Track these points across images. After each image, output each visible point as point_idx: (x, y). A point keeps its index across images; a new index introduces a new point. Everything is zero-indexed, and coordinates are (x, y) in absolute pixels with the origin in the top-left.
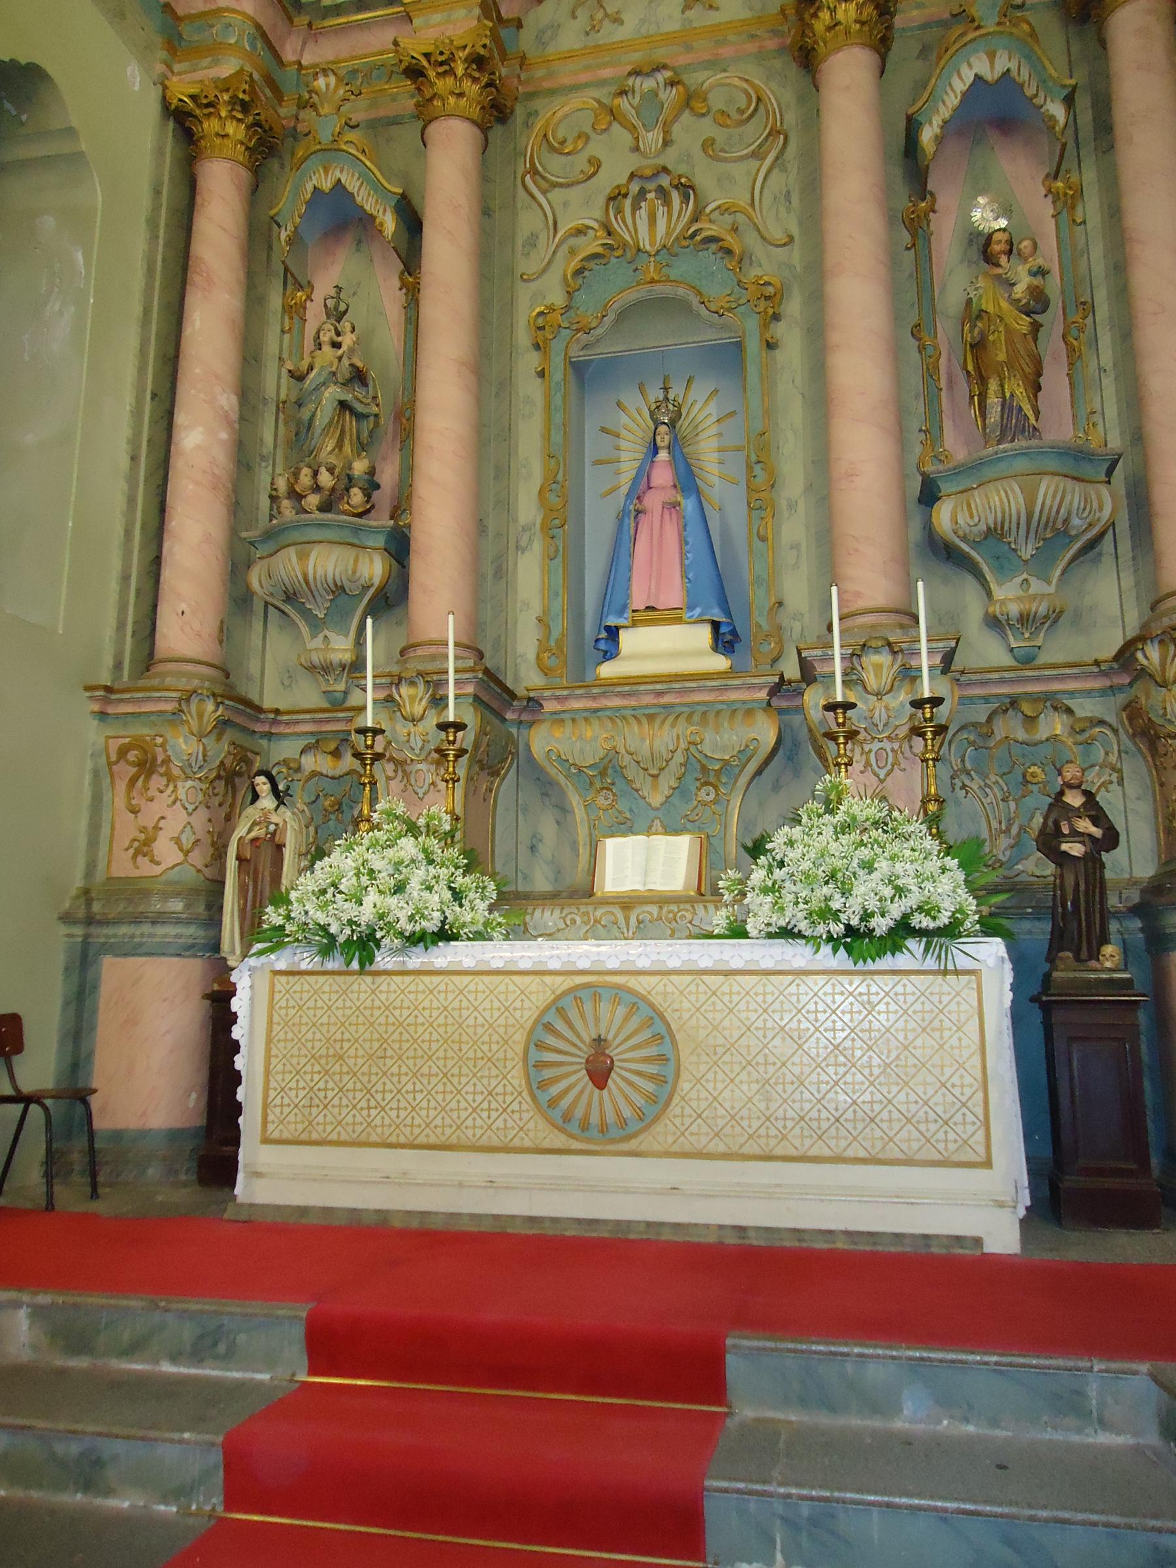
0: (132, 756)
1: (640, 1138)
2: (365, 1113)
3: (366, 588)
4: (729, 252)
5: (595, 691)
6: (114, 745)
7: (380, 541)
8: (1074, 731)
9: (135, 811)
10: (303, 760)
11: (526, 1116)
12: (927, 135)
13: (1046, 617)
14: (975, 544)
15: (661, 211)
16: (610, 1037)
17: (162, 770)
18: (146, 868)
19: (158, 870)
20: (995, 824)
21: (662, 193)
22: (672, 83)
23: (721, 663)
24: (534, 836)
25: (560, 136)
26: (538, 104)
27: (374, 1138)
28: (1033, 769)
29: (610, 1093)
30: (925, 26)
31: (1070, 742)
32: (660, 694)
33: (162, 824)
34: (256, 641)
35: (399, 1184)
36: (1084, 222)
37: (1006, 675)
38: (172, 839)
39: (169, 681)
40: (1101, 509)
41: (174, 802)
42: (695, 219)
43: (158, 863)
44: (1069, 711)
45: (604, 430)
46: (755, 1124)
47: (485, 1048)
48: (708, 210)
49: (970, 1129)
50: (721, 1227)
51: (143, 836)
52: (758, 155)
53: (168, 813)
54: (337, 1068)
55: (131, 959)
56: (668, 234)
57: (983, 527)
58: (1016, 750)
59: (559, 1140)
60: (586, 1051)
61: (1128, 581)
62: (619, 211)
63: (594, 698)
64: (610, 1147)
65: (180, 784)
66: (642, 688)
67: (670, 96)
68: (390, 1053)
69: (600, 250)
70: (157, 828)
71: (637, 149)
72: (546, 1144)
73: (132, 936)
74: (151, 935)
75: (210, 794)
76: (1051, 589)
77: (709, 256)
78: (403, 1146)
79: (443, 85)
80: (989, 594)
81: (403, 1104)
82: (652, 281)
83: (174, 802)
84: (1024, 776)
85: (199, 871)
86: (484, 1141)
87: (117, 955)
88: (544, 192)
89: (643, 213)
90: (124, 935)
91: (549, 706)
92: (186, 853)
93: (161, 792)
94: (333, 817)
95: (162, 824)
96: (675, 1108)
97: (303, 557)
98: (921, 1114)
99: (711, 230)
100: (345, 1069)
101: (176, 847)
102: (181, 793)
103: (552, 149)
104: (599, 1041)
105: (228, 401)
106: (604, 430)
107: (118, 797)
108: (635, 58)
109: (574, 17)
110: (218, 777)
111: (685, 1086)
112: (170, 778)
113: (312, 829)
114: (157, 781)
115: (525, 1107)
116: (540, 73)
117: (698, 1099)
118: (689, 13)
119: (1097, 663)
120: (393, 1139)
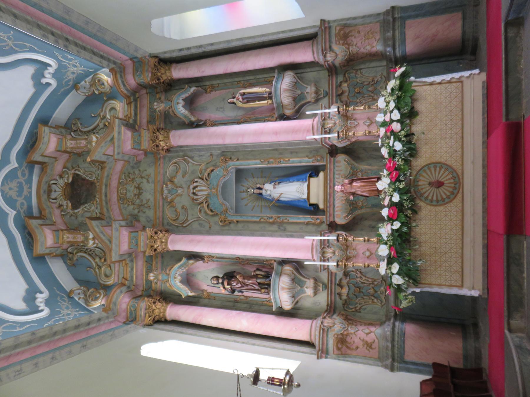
0: (340, 346)
1: (459, 173)
2: (453, 254)
3: (293, 273)
4: (212, 171)
5: (328, 205)
6: (336, 352)
7: (280, 267)
8: (346, 81)
9: (357, 348)
10: (343, 299)
11: (452, 205)
12: (193, 119)
13: (316, 88)
14: (296, 105)
15: (199, 188)
16: (429, 181)
17: (345, 336)
19: (376, 341)
20: (371, 100)
21: (195, 188)
22: (167, 185)
23: (321, 174)
24: (369, 227)
25: (174, 216)
26: (165, 222)
27: (460, 251)
28: (356, 91)
29: (444, 181)
30: (165, 123)
31: (349, 82)
32: (330, 187)
33: (362, 338)
35: (474, 242)
36: (218, 84)
37: (331, 97)
38: (367, 336)
40: (290, 75)
41: (355, 334)
42: (203, 179)
43: (374, 341)
44: (341, 82)
45: (252, 210)
46: (453, 141)
47: (432, 217)
48: (200, 176)
49: (452, 87)
50: (483, 148)
51: (366, 345)
52: (188, 163)
53: (358, 336)
54: (439, 263)
55: (406, 349)
56: (205, 186)
57: (293, 102)
58: (351, 95)
59: (460, 196)
60: (434, 189)
61: (309, 70)
62: (196, 200)
63: (330, 206)
64: (461, 180)
65: (349, 332)
66: (328, 192)
67: (170, 186)
68: (434, 246)
69: (206, 204)
70: (363, 340)
71: (181, 195)
72: (461, 199)
73: (398, 348)
74: (398, 341)
75: (353, 324)
76: (309, 87)
77: (212, 175)
78: (463, 242)
80: (309, 102)
81: (449, 242)
82: (217, 190)
83: (355, 334)
84: (358, 93)
85: (377, 329)
86: (460, 217)
87: (404, 354)
88: (188, 221)
89: (199, 193)
90: (398, 351)
91: (332, 220)
93: (351, 338)
94: (361, 290)
95: (362, 338)
96: (449, 163)
98: (449, 99)
99: (206, 174)
100: (439, 260)
101: (369, 335)
102: (353, 331)
103: (177, 219)
104: (430, 184)
106: (252, 210)
108: (158, 195)
109: (145, 212)
110: (348, 321)
111: (443, 160)
112: (347, 335)
113: (365, 297)
114: (348, 339)
115: (449, 205)
116: (158, 221)
117: (446, 157)
118: (150, 181)
119: (329, 76)
120: (461, 245)
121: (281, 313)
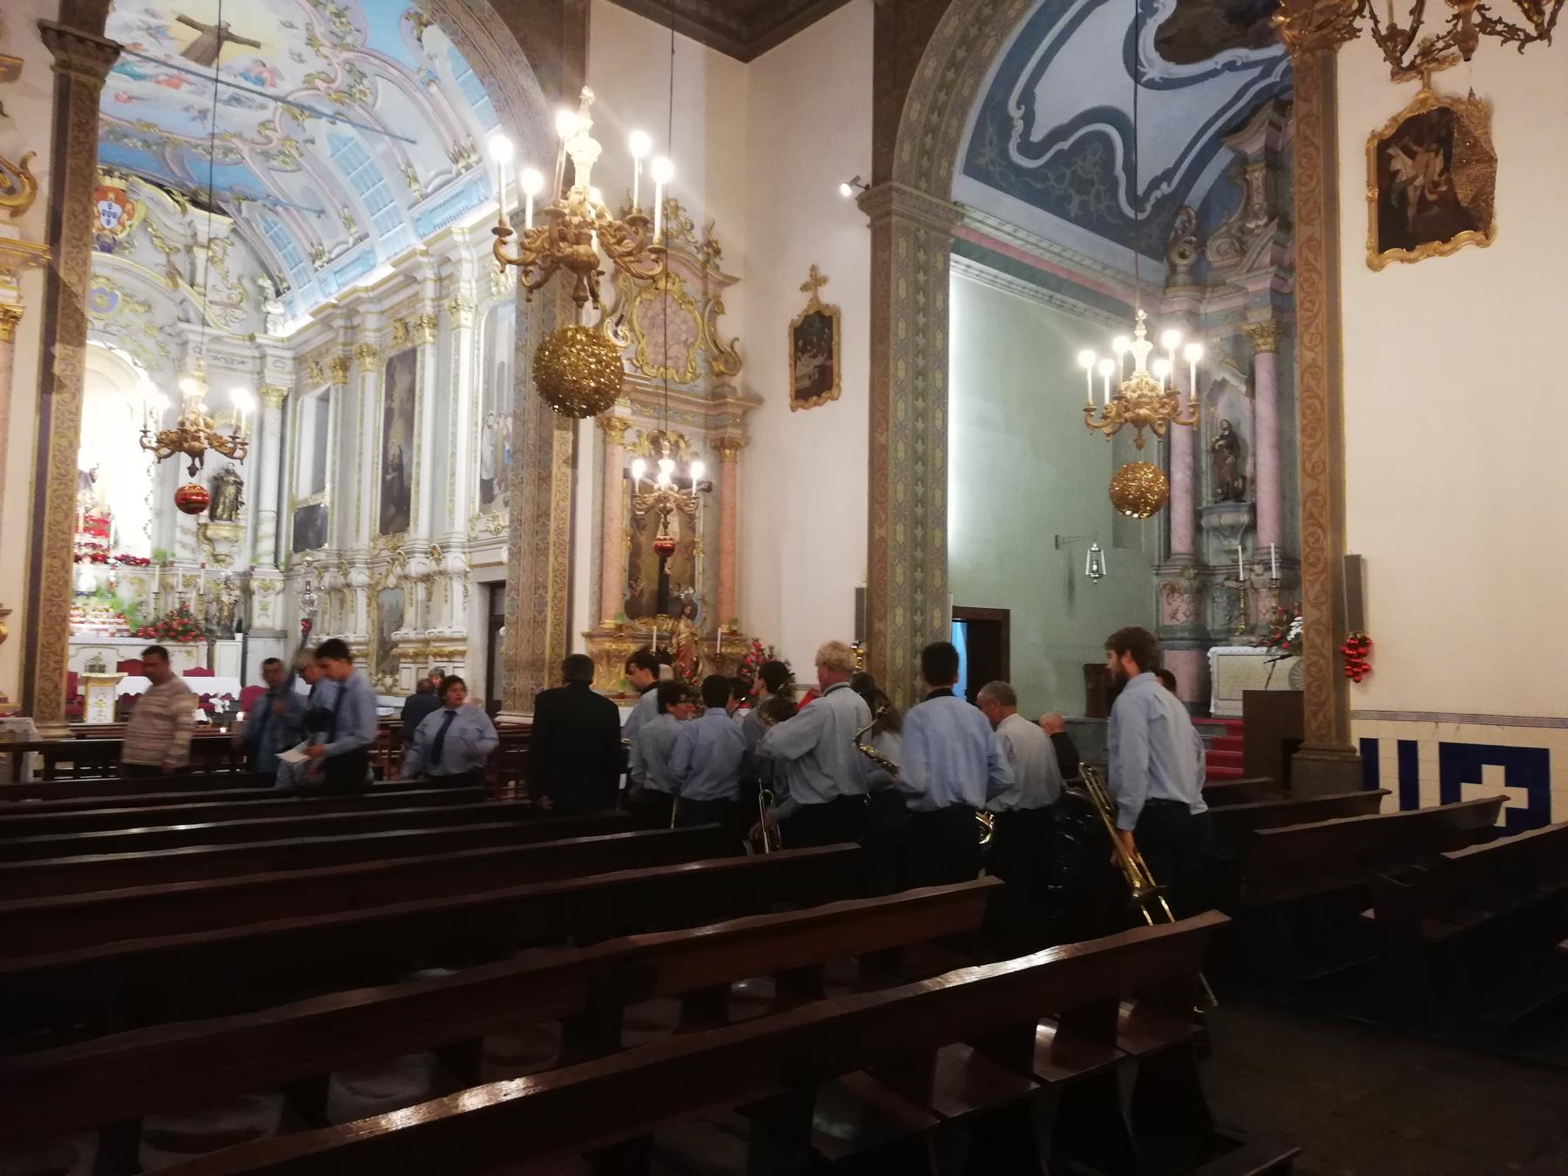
0: (1168, 587)
7: (1246, 509)
9: (1170, 604)
18: (1175, 622)
34: (1205, 540)
39: (1178, 562)
79: (1260, 341)
92: (1188, 617)
97: (1220, 517)
105: (1189, 459)
107: (1163, 600)
114: (1176, 595)
121: (1197, 515)
